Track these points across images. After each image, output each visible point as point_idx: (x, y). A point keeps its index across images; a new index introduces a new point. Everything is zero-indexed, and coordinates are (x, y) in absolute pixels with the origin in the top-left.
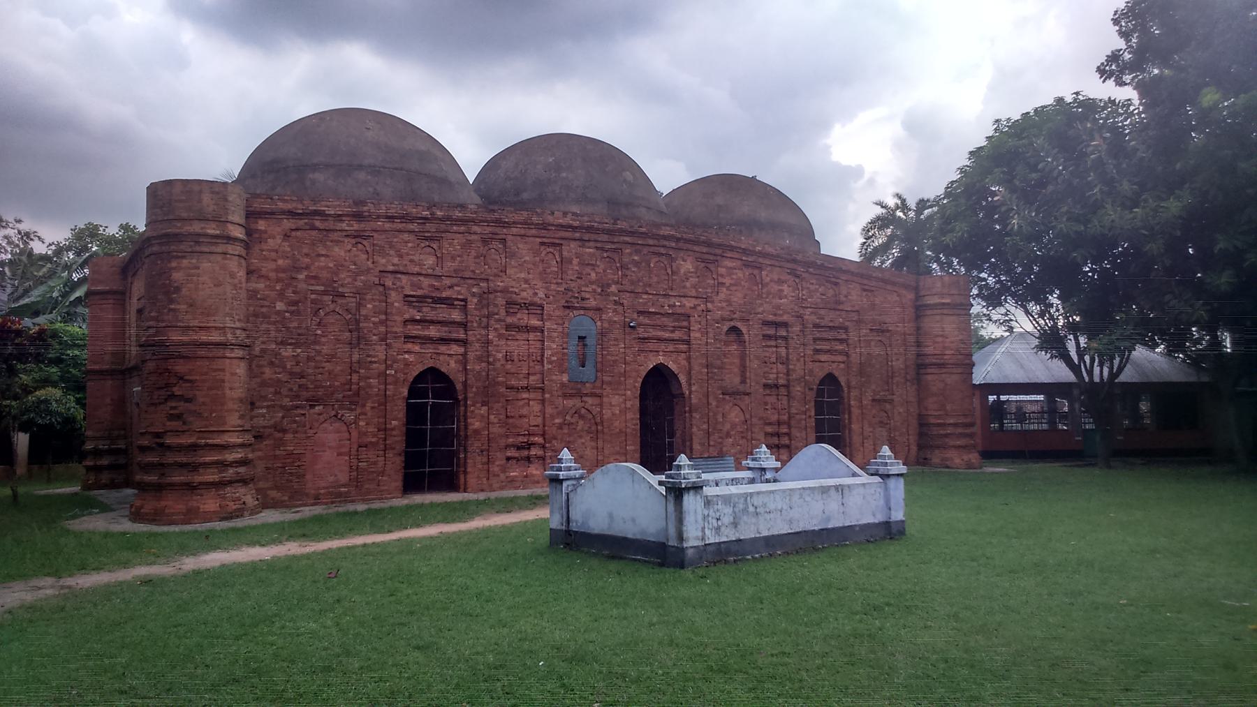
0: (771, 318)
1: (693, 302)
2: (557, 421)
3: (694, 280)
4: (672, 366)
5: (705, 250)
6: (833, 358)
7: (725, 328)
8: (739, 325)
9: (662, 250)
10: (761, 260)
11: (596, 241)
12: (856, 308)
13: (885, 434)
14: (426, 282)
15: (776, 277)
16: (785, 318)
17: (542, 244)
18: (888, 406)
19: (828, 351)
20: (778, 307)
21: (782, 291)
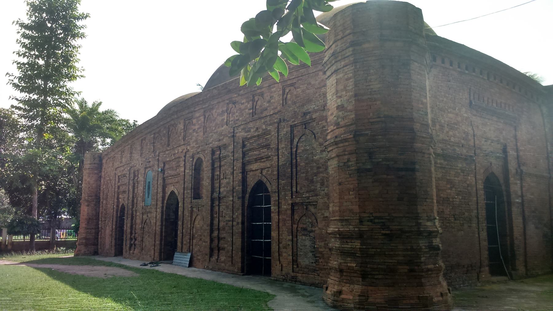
0: (216, 144)
1: (183, 147)
2: (140, 226)
3: (183, 134)
4: (176, 192)
5: (187, 112)
6: (262, 165)
7: (195, 161)
8: (201, 156)
9: (172, 122)
10: (212, 103)
11: (154, 130)
12: (279, 108)
13: (308, 243)
14: (122, 169)
15: (220, 111)
16: (226, 140)
17: (142, 140)
18: (312, 209)
19: (256, 160)
20: (221, 134)
21: (223, 119)
